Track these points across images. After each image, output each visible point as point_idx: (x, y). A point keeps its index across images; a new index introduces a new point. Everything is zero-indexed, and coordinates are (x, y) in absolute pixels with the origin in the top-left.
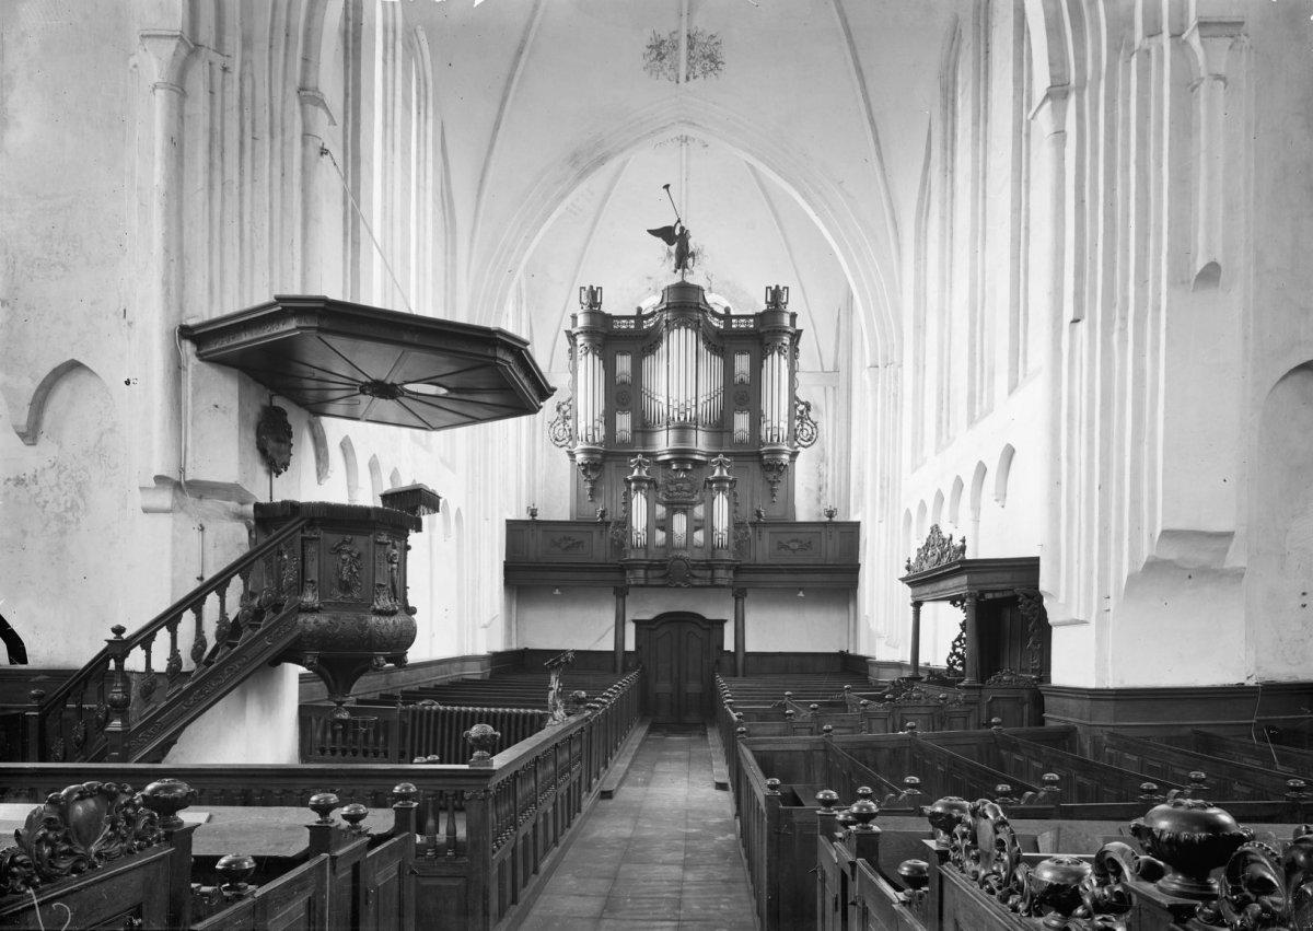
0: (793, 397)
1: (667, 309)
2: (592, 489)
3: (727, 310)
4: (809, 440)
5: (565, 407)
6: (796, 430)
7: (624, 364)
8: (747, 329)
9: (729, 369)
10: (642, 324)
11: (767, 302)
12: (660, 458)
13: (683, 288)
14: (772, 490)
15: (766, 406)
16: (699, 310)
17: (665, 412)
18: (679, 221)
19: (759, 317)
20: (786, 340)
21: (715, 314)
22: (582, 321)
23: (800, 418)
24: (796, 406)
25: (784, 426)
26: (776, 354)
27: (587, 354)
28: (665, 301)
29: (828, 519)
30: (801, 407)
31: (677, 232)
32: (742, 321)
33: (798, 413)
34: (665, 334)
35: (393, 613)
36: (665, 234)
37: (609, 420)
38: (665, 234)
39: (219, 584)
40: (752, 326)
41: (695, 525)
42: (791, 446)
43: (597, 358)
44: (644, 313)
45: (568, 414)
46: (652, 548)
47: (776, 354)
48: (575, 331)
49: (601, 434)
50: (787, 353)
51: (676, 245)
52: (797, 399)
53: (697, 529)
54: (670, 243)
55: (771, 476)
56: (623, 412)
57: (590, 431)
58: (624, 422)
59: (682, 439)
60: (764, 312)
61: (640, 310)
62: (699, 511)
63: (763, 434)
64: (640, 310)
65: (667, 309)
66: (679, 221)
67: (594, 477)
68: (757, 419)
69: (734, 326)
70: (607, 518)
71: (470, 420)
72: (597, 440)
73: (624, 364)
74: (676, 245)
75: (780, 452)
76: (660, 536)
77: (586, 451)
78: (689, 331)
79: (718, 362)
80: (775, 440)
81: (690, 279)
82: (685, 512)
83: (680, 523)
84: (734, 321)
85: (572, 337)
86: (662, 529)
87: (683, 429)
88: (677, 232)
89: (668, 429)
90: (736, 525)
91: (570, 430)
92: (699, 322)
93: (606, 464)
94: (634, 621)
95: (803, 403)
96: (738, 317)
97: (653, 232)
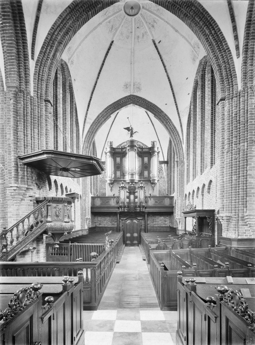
1: (128, 147)
2: (111, 189)
7: (118, 159)
8: (147, 151)
12: (127, 182)
13: (132, 142)
15: (151, 169)
16: (136, 146)
19: (150, 148)
22: (109, 149)
28: (128, 145)
31: (130, 128)
34: (128, 152)
35: (69, 222)
36: (128, 129)
37: (115, 173)
38: (128, 129)
39: (28, 217)
41: (136, 197)
46: (125, 203)
48: (106, 152)
49: (113, 176)
53: (136, 198)
54: (129, 131)
55: (153, 185)
57: (111, 175)
58: (118, 173)
59: (132, 177)
63: (151, 175)
65: (128, 147)
68: (149, 173)
70: (115, 196)
71: (83, 176)
73: (118, 159)
76: (128, 200)
79: (140, 159)
80: (154, 177)
82: (133, 194)
83: (132, 197)
85: (106, 153)
87: (132, 175)
88: (130, 128)
90: (146, 197)
93: (115, 183)
97: (125, 129)
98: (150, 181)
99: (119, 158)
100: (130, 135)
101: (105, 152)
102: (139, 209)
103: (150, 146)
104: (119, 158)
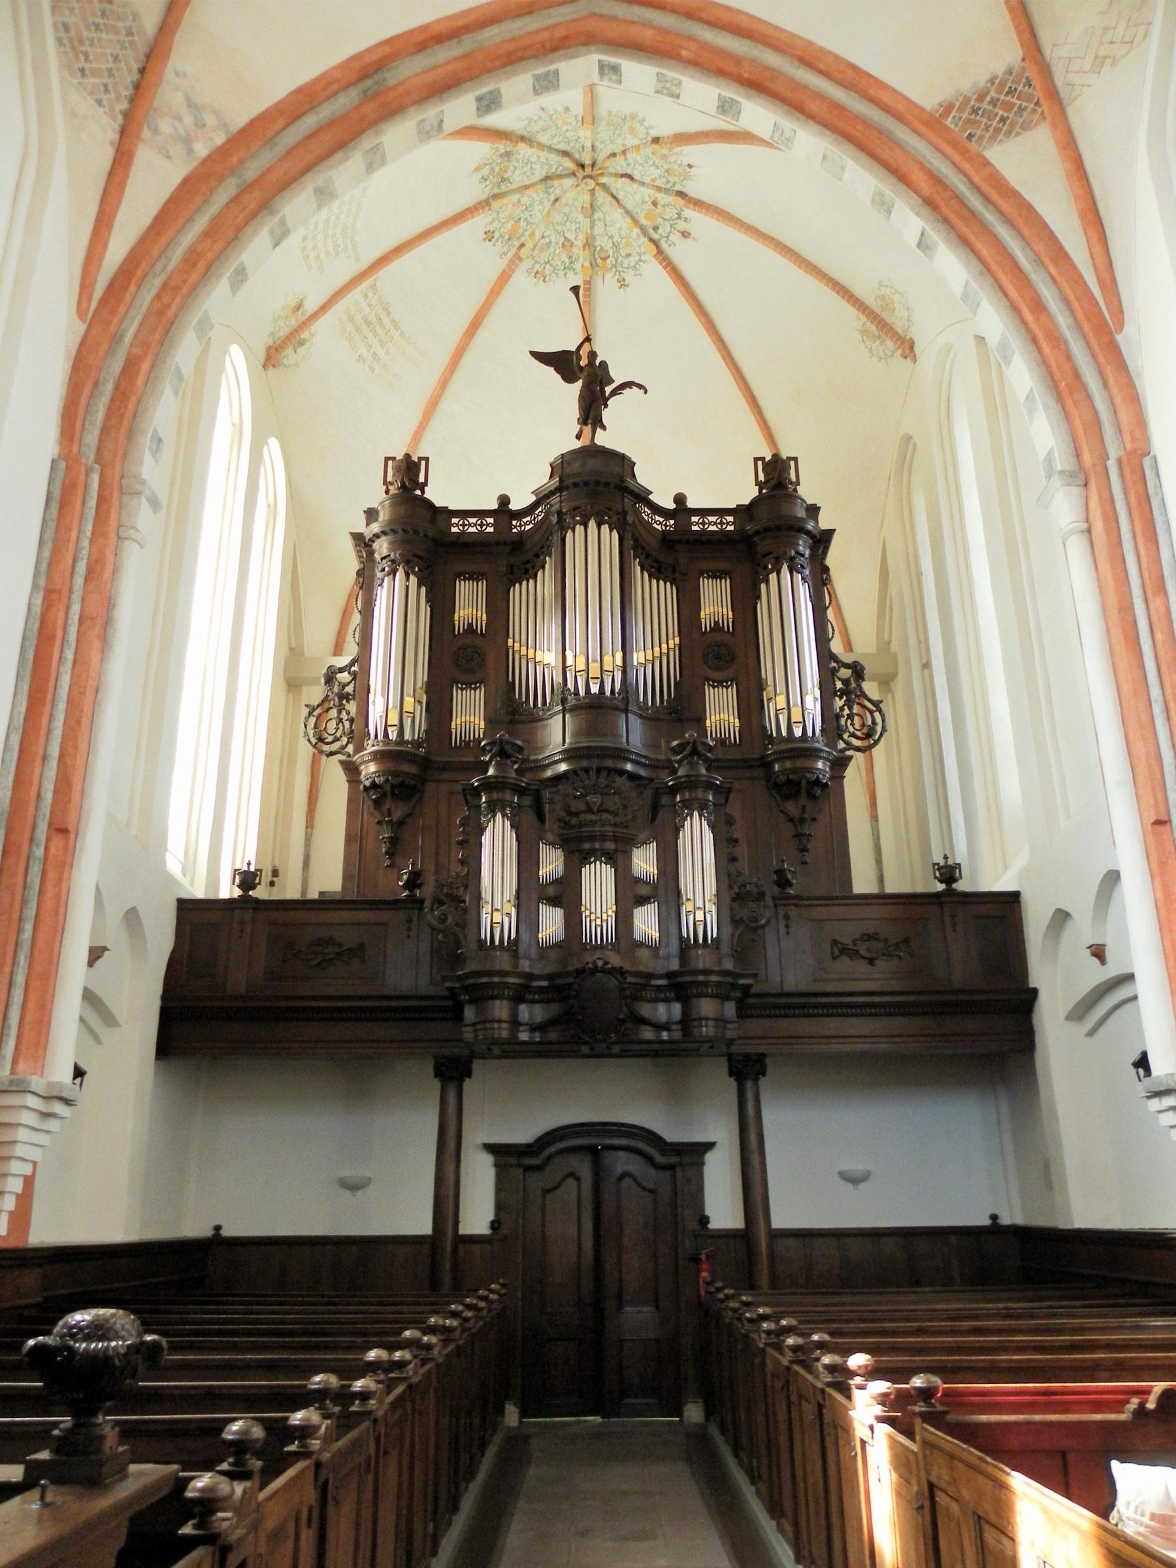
0: (825, 655)
2: (394, 841)
3: (680, 499)
4: (868, 736)
5: (344, 677)
6: (838, 717)
8: (723, 532)
9: (689, 605)
10: (511, 527)
11: (758, 483)
14: (798, 836)
15: (770, 668)
17: (558, 679)
18: (588, 339)
20: (803, 546)
21: (657, 509)
23: (843, 693)
24: (834, 672)
25: (813, 704)
26: (785, 569)
27: (393, 572)
29: (941, 887)
30: (845, 673)
32: (713, 519)
33: (839, 685)
40: (731, 528)
42: (832, 744)
43: (413, 580)
44: (514, 506)
45: (349, 689)
47: (785, 569)
50: (807, 572)
51: (580, 383)
52: (833, 657)
53: (642, 901)
54: (569, 378)
55: (792, 808)
56: (469, 685)
57: (394, 719)
60: (754, 502)
61: (504, 501)
62: (644, 862)
64: (504, 501)
66: (588, 339)
67: (397, 815)
69: (695, 528)
72: (407, 736)
74: (580, 383)
75: (814, 753)
77: (378, 756)
78: (605, 528)
79: (667, 592)
81: (603, 439)
82: (611, 859)
84: (694, 519)
86: (554, 902)
88: (583, 363)
89: (564, 711)
91: (352, 721)
92: (625, 513)
93: (430, 787)
94: (491, 1148)
95: (847, 666)
96: (704, 512)
98: (766, 764)
99: (482, 586)
100: (573, 411)
101: (358, 538)
102: (677, 1008)
103: (744, 492)
104: (482, 586)
